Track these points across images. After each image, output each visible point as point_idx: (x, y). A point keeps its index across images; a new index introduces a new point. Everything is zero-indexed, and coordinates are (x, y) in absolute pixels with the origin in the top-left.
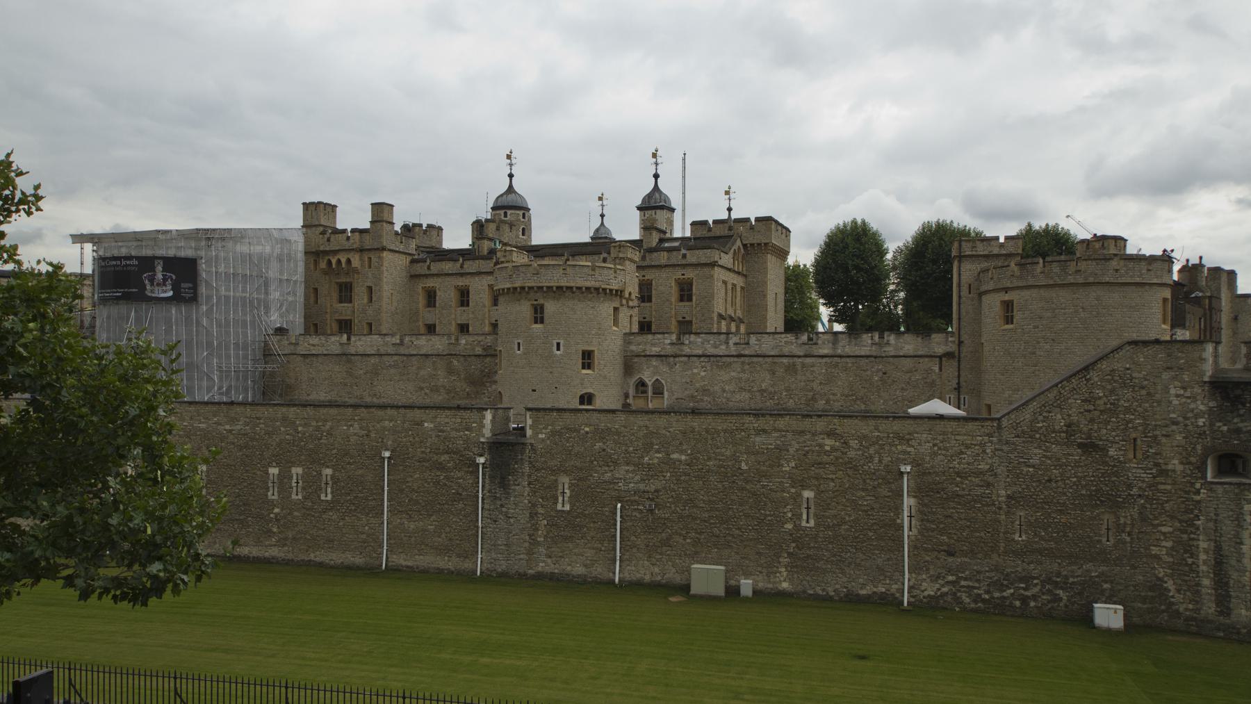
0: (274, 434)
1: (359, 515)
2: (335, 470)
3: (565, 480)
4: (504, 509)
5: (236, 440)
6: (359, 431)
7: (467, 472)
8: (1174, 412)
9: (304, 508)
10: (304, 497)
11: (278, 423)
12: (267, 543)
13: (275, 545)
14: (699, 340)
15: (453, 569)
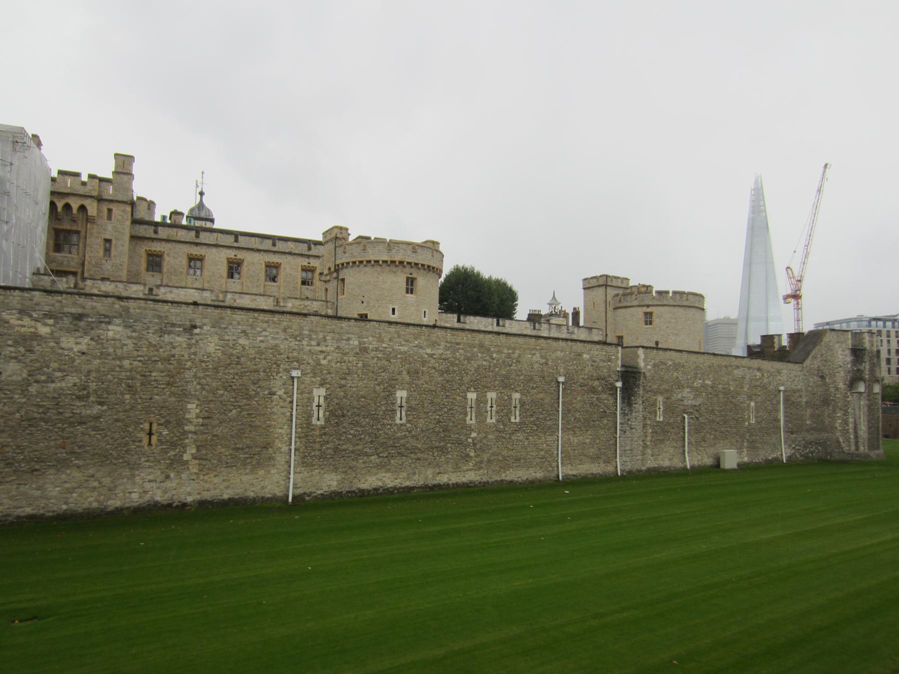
0: (473, 360)
1: (539, 434)
2: (522, 394)
3: (660, 399)
4: (630, 422)
5: (437, 365)
6: (540, 359)
7: (610, 394)
8: (840, 362)
9: (496, 430)
10: (498, 421)
11: (476, 350)
12: (465, 468)
13: (471, 470)
14: (476, 321)
15: (601, 473)
